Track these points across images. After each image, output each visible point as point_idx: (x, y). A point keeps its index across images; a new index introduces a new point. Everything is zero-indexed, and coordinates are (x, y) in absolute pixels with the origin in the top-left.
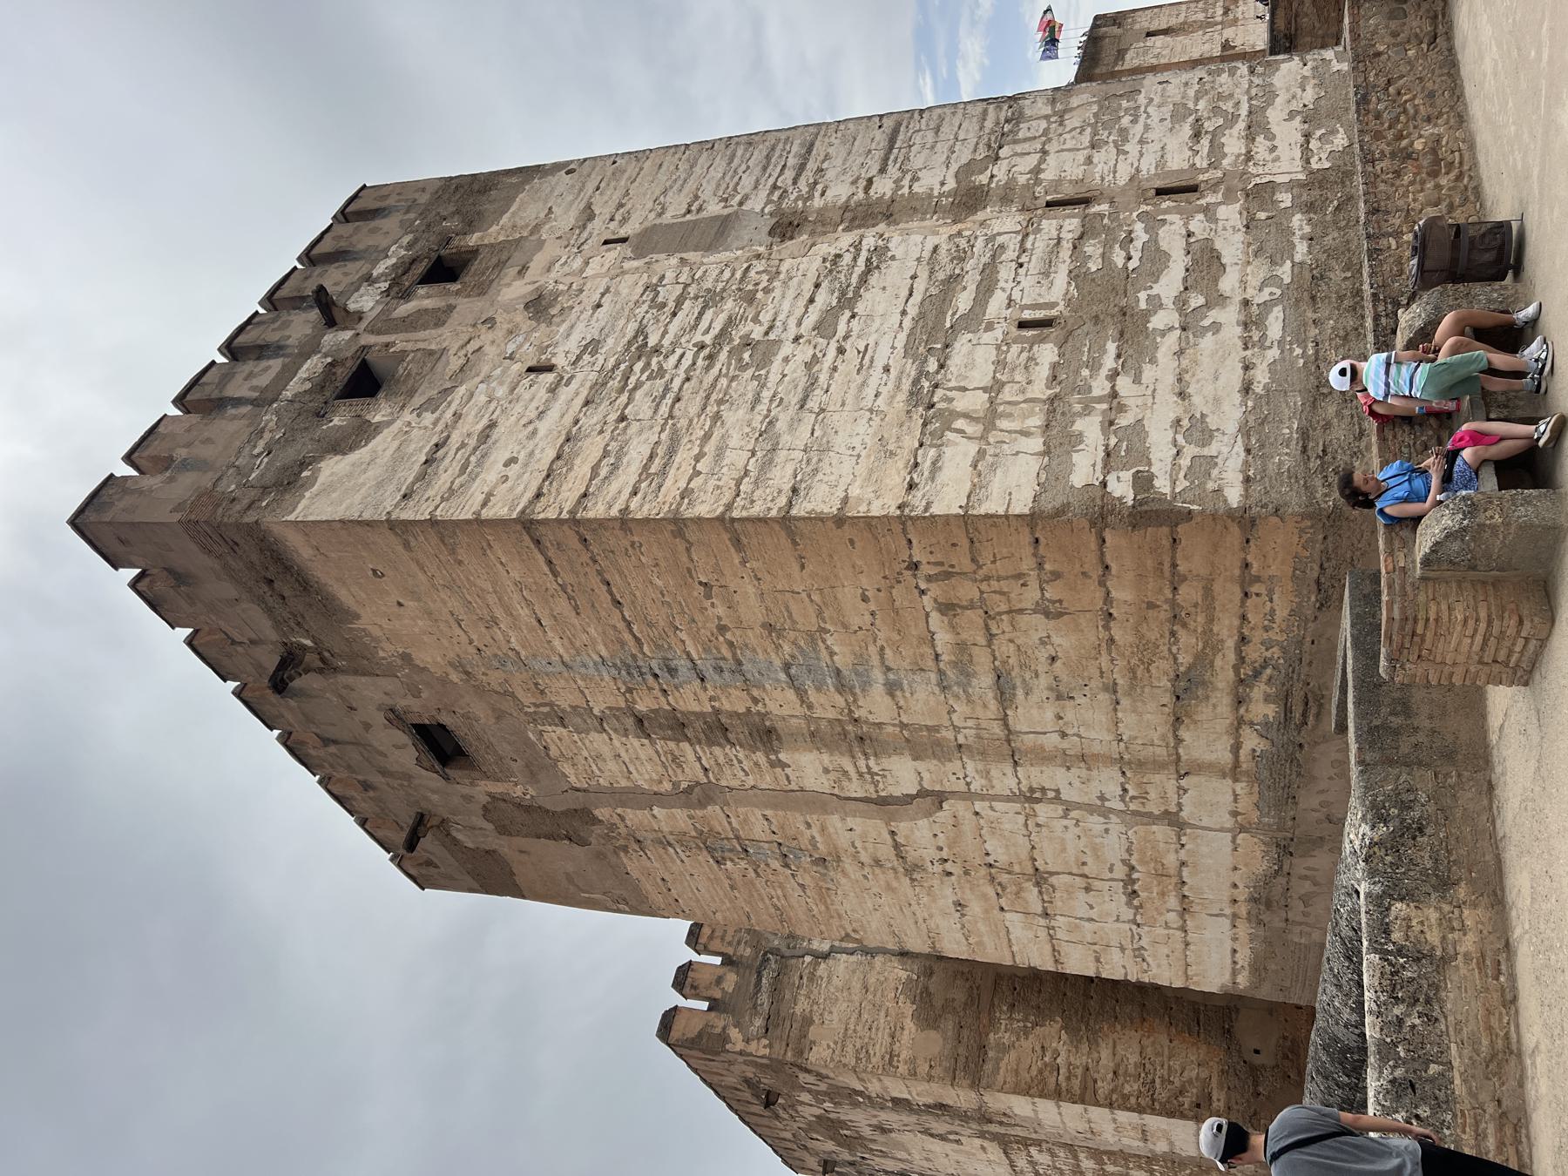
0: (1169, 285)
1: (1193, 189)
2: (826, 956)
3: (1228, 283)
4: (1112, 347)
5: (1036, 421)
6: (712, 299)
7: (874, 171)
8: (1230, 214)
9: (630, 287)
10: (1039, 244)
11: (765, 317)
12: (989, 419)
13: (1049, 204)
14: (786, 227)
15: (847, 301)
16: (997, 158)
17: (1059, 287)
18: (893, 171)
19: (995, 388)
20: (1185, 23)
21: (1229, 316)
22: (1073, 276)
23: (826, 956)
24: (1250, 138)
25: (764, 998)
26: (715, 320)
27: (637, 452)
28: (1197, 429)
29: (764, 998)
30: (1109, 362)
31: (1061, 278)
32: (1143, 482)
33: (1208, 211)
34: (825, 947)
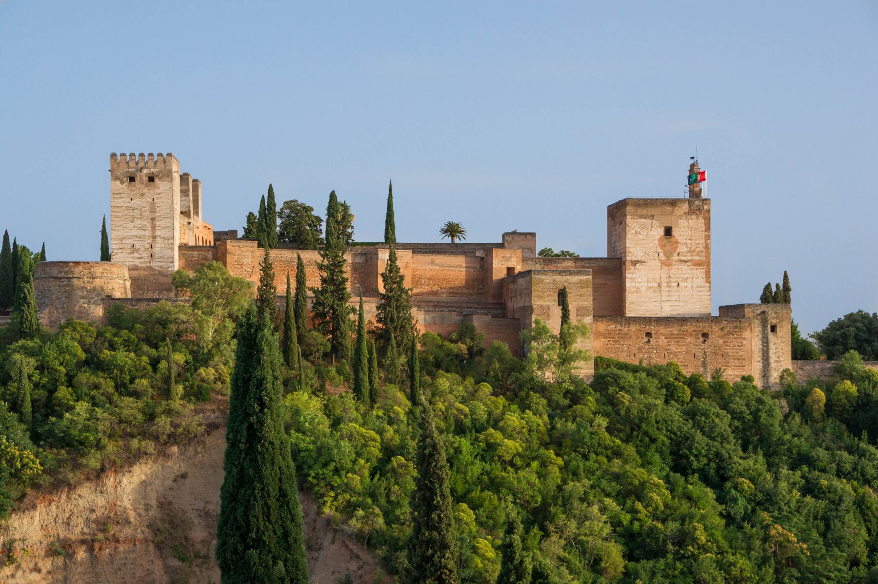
6: (141, 214)
9: (145, 204)
14: (153, 219)
15: (140, 229)
17: (138, 247)
20: (677, 242)
26: (137, 216)
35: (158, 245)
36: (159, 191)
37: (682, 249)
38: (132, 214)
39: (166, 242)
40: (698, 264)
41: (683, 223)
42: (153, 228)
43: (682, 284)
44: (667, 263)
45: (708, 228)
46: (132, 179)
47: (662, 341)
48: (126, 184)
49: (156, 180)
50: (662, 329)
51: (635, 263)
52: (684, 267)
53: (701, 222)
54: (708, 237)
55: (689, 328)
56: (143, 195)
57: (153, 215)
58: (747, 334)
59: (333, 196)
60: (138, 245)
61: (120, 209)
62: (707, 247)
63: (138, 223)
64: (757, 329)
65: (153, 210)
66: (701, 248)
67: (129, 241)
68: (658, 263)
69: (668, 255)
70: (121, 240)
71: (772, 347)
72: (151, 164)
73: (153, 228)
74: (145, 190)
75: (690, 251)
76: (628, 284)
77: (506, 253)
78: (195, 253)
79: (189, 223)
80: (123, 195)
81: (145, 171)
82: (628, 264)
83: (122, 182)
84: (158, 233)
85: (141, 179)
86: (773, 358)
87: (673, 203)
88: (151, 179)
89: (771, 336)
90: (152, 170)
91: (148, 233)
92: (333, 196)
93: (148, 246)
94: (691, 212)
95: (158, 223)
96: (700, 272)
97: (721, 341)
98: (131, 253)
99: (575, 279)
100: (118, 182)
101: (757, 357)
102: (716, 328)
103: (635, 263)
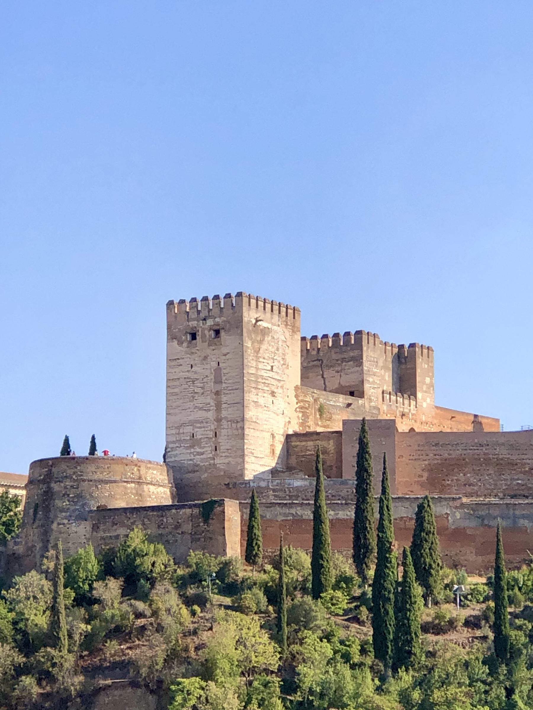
0: (198, 450)
1: (216, 450)
2: (323, 377)
3: (198, 457)
4: (188, 445)
5: (178, 439)
7: (228, 403)
8: (211, 455)
9: (207, 373)
10: (208, 432)
11: (199, 398)
12: (179, 434)
13: (216, 433)
14: (217, 393)
15: (201, 409)
16: (228, 422)
17: (199, 437)
18: (229, 406)
19: (183, 433)
21: (192, 457)
22: (201, 439)
23: (323, 377)
24: (225, 456)
25: (312, 363)
26: (200, 390)
27: (176, 390)
28: (175, 456)
29: (312, 363)
30: (186, 445)
31: (200, 437)
32: (169, 452)
33: (211, 453)
34: (325, 376)
35: (224, 432)
36: (225, 350)
38: (192, 388)
39: (234, 425)
42: (218, 407)
46: (194, 336)
48: (185, 344)
49: (222, 333)
56: (206, 358)
57: (218, 387)
60: (199, 434)
61: (177, 383)
63: (200, 400)
65: (218, 381)
67: (189, 429)
70: (178, 428)
72: (216, 311)
73: (218, 407)
74: (209, 351)
78: (310, 443)
79: (349, 405)
80: (181, 361)
81: (210, 322)
83: (180, 343)
84: (224, 414)
85: (204, 335)
88: (217, 332)
90: (217, 320)
91: (211, 415)
93: (211, 434)
95: (224, 399)
98: (192, 446)
100: (175, 342)
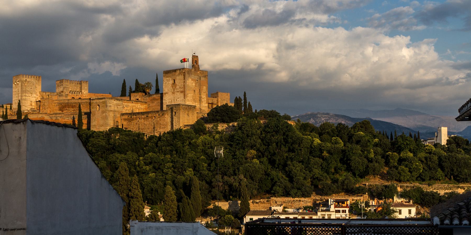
37: (178, 87)
40: (182, 92)
41: (178, 77)
43: (178, 100)
44: (173, 93)
45: (184, 79)
47: (142, 120)
50: (143, 116)
51: (165, 93)
52: (178, 94)
53: (183, 76)
54: (184, 82)
55: (150, 115)
58: (166, 116)
59: (137, 81)
62: (184, 86)
64: (170, 114)
66: (183, 86)
68: (171, 93)
69: (174, 90)
71: (174, 120)
75: (180, 88)
76: (164, 102)
77: (136, 94)
82: (164, 94)
86: (174, 124)
87: (175, 71)
89: (174, 116)
92: (137, 81)
94: (180, 74)
96: (182, 95)
97: (159, 119)
99: (101, 101)
101: (170, 124)
102: (157, 115)
103: (165, 93)
